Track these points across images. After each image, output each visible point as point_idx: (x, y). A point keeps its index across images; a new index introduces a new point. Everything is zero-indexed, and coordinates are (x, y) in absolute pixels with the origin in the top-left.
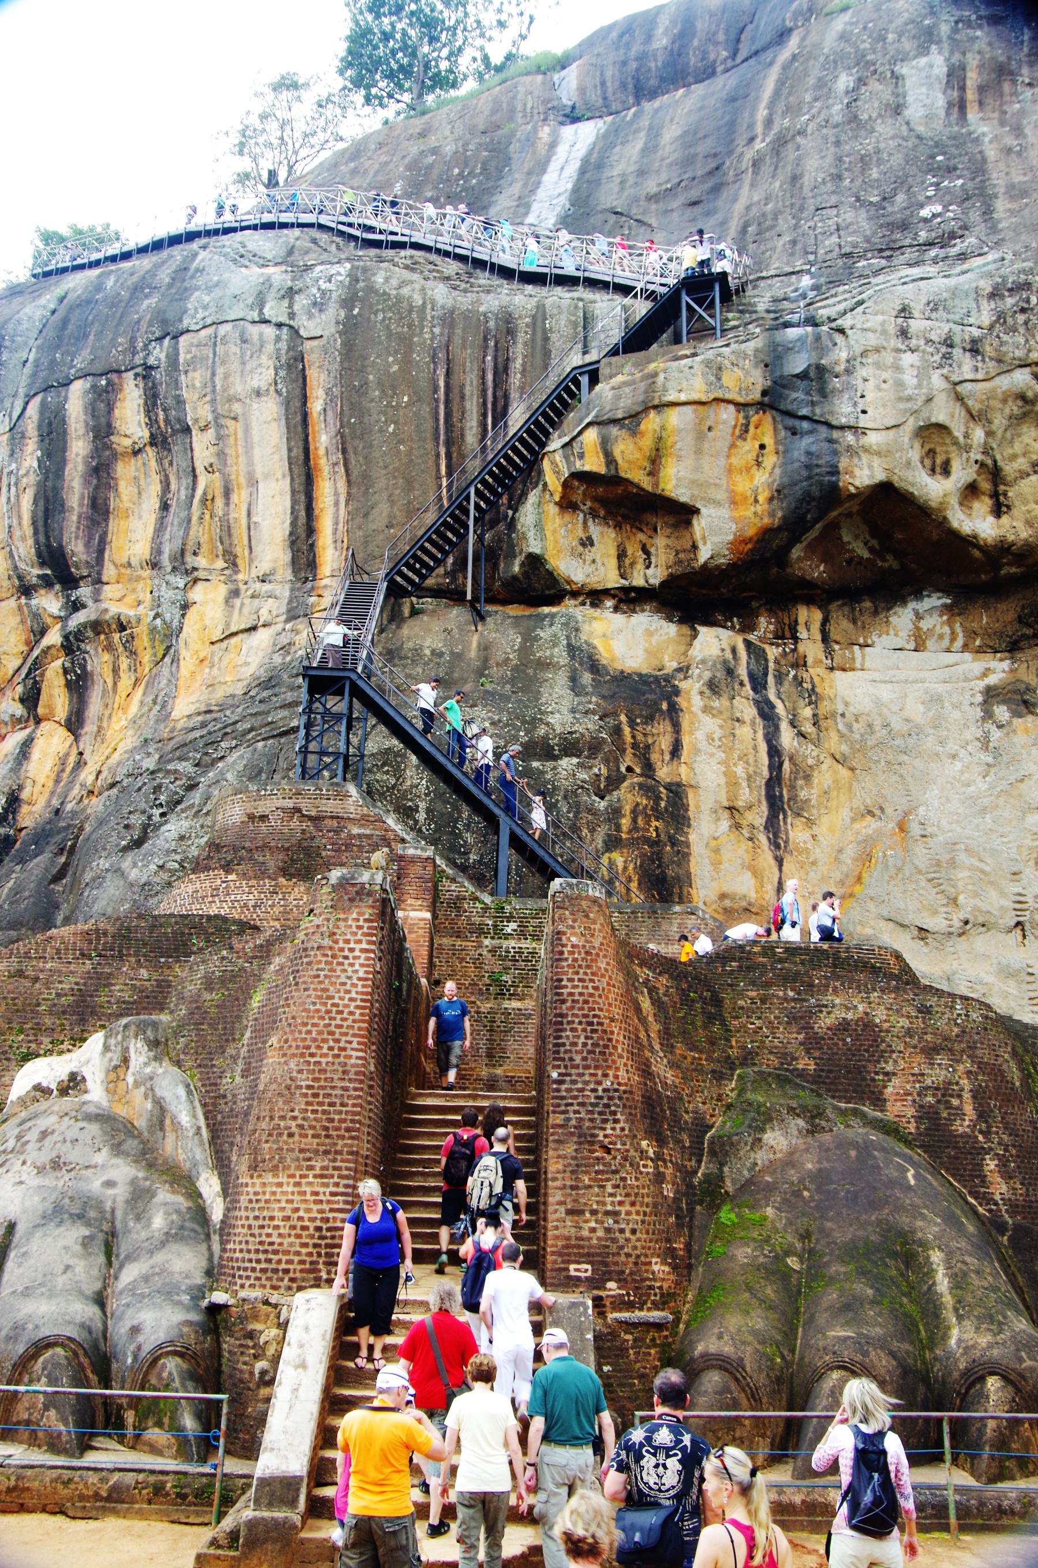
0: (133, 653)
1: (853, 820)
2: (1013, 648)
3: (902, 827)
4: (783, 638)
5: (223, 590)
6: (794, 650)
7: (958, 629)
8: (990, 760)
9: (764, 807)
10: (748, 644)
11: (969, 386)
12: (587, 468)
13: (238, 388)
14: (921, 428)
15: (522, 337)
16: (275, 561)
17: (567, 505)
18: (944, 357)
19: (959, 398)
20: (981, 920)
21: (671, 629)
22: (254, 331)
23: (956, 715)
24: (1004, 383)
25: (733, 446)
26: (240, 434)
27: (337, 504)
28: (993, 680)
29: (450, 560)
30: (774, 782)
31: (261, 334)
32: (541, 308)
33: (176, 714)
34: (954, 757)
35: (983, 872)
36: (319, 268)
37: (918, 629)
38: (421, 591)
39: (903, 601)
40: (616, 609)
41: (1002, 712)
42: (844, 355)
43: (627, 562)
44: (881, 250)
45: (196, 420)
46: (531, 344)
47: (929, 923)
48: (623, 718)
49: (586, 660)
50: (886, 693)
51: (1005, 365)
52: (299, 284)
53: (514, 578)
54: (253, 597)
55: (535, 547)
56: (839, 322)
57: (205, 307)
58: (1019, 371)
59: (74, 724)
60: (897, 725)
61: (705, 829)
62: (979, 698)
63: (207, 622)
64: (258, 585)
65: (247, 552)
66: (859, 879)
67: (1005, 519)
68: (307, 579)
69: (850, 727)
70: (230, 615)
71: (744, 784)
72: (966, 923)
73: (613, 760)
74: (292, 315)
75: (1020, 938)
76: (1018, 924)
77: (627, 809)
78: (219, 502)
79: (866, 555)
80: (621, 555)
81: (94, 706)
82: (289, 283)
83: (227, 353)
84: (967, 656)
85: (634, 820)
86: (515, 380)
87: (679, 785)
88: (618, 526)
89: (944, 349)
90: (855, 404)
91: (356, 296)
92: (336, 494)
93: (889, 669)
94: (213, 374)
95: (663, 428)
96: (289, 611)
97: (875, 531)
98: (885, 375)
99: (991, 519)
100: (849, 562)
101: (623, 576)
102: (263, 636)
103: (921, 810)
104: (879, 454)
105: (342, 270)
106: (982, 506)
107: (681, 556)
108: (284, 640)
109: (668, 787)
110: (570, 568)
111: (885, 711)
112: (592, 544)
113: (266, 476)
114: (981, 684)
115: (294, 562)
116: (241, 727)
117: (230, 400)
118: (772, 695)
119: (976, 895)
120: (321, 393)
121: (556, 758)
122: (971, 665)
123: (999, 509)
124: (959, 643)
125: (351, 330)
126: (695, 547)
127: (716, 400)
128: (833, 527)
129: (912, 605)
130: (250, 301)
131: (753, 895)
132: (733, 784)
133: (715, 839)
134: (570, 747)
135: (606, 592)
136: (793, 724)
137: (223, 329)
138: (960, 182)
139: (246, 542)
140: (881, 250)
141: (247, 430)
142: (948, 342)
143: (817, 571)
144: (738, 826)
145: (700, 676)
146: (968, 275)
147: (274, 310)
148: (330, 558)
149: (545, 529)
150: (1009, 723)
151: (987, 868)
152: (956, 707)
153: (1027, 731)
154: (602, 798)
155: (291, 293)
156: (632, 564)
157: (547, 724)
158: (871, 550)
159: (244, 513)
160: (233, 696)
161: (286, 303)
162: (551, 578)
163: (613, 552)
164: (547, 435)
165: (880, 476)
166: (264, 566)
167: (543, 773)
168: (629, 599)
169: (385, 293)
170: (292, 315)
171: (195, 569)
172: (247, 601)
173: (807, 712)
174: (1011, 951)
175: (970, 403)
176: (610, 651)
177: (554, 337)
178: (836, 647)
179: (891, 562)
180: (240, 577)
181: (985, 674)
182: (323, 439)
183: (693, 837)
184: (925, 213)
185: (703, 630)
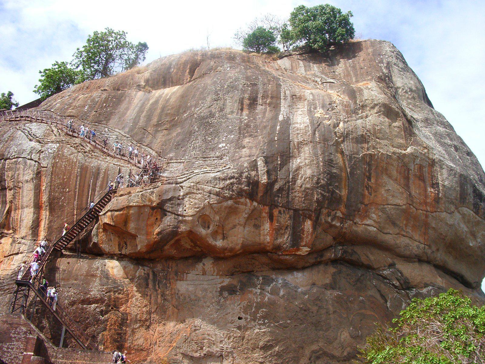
2: (232, 274)
4: (163, 270)
5: (11, 240)
6: (167, 274)
7: (216, 270)
8: (219, 308)
10: (154, 272)
11: (215, 205)
12: (107, 222)
13: (21, 178)
14: (201, 216)
15: (101, 175)
16: (27, 233)
17: (105, 230)
18: (208, 196)
19: (212, 208)
21: (132, 267)
22: (29, 161)
23: (211, 295)
24: (225, 204)
25: (149, 218)
26: (21, 192)
27: (46, 218)
28: (224, 284)
29: (74, 240)
31: (30, 163)
32: (108, 166)
34: (208, 307)
35: (212, 340)
36: (50, 144)
37: (204, 269)
38: (66, 248)
39: (201, 261)
40: (117, 260)
41: (226, 294)
42: (182, 194)
43: (121, 246)
44: (204, 158)
45: (9, 187)
46: (103, 178)
48: (112, 293)
49: (106, 276)
50: (191, 288)
51: (226, 199)
52: (43, 149)
53: (90, 248)
54: (19, 243)
55: (95, 240)
56: (182, 184)
57: (16, 152)
58: (230, 201)
60: (193, 297)
62: (219, 289)
63: (4, 250)
64: (21, 240)
65: (19, 229)
67: (225, 241)
68: (35, 240)
69: (179, 297)
70: (11, 249)
73: (108, 305)
74: (39, 159)
75: (222, 359)
78: (13, 212)
79: (189, 247)
80: (119, 245)
82: (40, 149)
83: (19, 168)
84: (218, 277)
86: (97, 189)
87: (127, 314)
88: (119, 237)
89: (208, 194)
90: (183, 208)
91: (57, 156)
92: (46, 215)
93: (193, 280)
94: (15, 174)
95: (129, 213)
96: (28, 250)
97: (192, 241)
98: (192, 200)
99: (221, 240)
100: (184, 250)
101: (119, 251)
102: (20, 256)
104: (188, 223)
105: (56, 147)
106: (220, 237)
107: (133, 247)
108: (24, 259)
109: (123, 314)
110: (105, 247)
111: (190, 293)
112: (111, 241)
113: (27, 206)
114: (220, 285)
115: (32, 233)
116: (6, 287)
117: (18, 182)
118: (157, 288)
119: (209, 347)
120: (45, 184)
121: (91, 304)
122: (218, 280)
123: (224, 238)
124: (215, 273)
125: (54, 165)
126: (137, 245)
127: (144, 206)
128: (179, 240)
129: (202, 262)
130: (28, 152)
133: (136, 329)
134: (96, 301)
135: (115, 254)
136: (162, 296)
137: (20, 159)
138: (232, 136)
139: (19, 226)
140: (204, 158)
141: (22, 192)
142: (210, 192)
143: (173, 252)
145: (137, 282)
146: (218, 173)
147: (35, 156)
148: (42, 234)
149: (98, 237)
150: (227, 297)
151: (213, 339)
152: (210, 292)
153: (231, 300)
154: (103, 316)
155: (40, 152)
156: (123, 247)
157: (90, 294)
158: (191, 246)
159: (19, 217)
160: (8, 275)
161: (38, 155)
162: (100, 248)
163: (117, 244)
164: (103, 207)
165: (188, 229)
166: (23, 234)
167: (86, 309)
168: (120, 258)
169: (66, 156)
170: (39, 159)
171: (3, 233)
172: (17, 245)
173: (167, 292)
175: (215, 209)
176: (113, 272)
177: (110, 177)
178: (179, 273)
179: (198, 249)
180: (16, 236)
181: (223, 282)
182: (45, 198)
184: (220, 146)
185: (140, 267)
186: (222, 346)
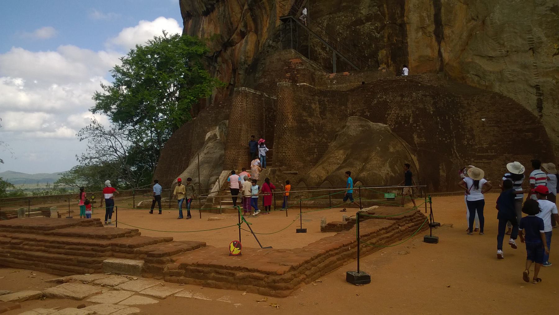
0: (265, 8)
1: (467, 23)
3: (484, 22)
9: (434, 26)
20: (514, 49)
30: (437, 16)
33: (277, 25)
35: (515, 32)
47: (492, 54)
59: (256, 32)
61: (413, 36)
66: (467, 44)
71: (426, 19)
72: (508, 52)
75: (532, 53)
76: (530, 49)
77: (386, 35)
81: (259, 27)
85: (389, 38)
103: (491, 15)
121: (364, 24)
131: (430, 55)
132: (422, 19)
144: (424, 33)
151: (516, 31)
157: (361, 13)
167: (359, 29)
174: (529, 59)
183: (409, 40)
186: (531, 36)
